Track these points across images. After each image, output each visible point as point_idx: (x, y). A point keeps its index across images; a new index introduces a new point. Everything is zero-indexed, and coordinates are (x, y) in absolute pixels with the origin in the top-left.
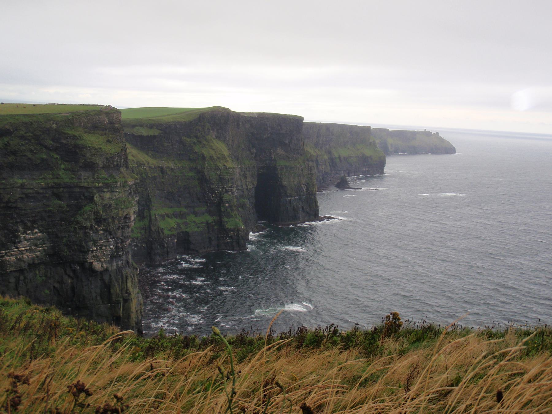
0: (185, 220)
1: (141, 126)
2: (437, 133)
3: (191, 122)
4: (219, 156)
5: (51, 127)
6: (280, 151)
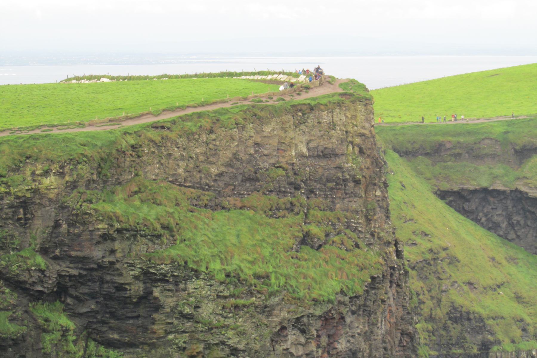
5: (36, 191)
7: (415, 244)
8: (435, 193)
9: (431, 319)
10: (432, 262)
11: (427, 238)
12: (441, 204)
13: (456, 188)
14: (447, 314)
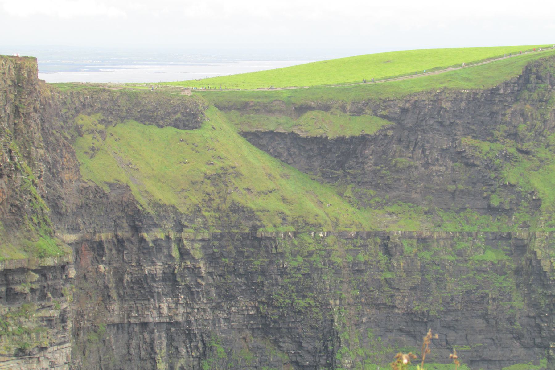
1: (327, 108)
3: (494, 91)
7: (213, 164)
8: (239, 133)
9: (218, 210)
10: (222, 175)
11: (221, 160)
12: (241, 140)
13: (253, 130)
14: (229, 207)
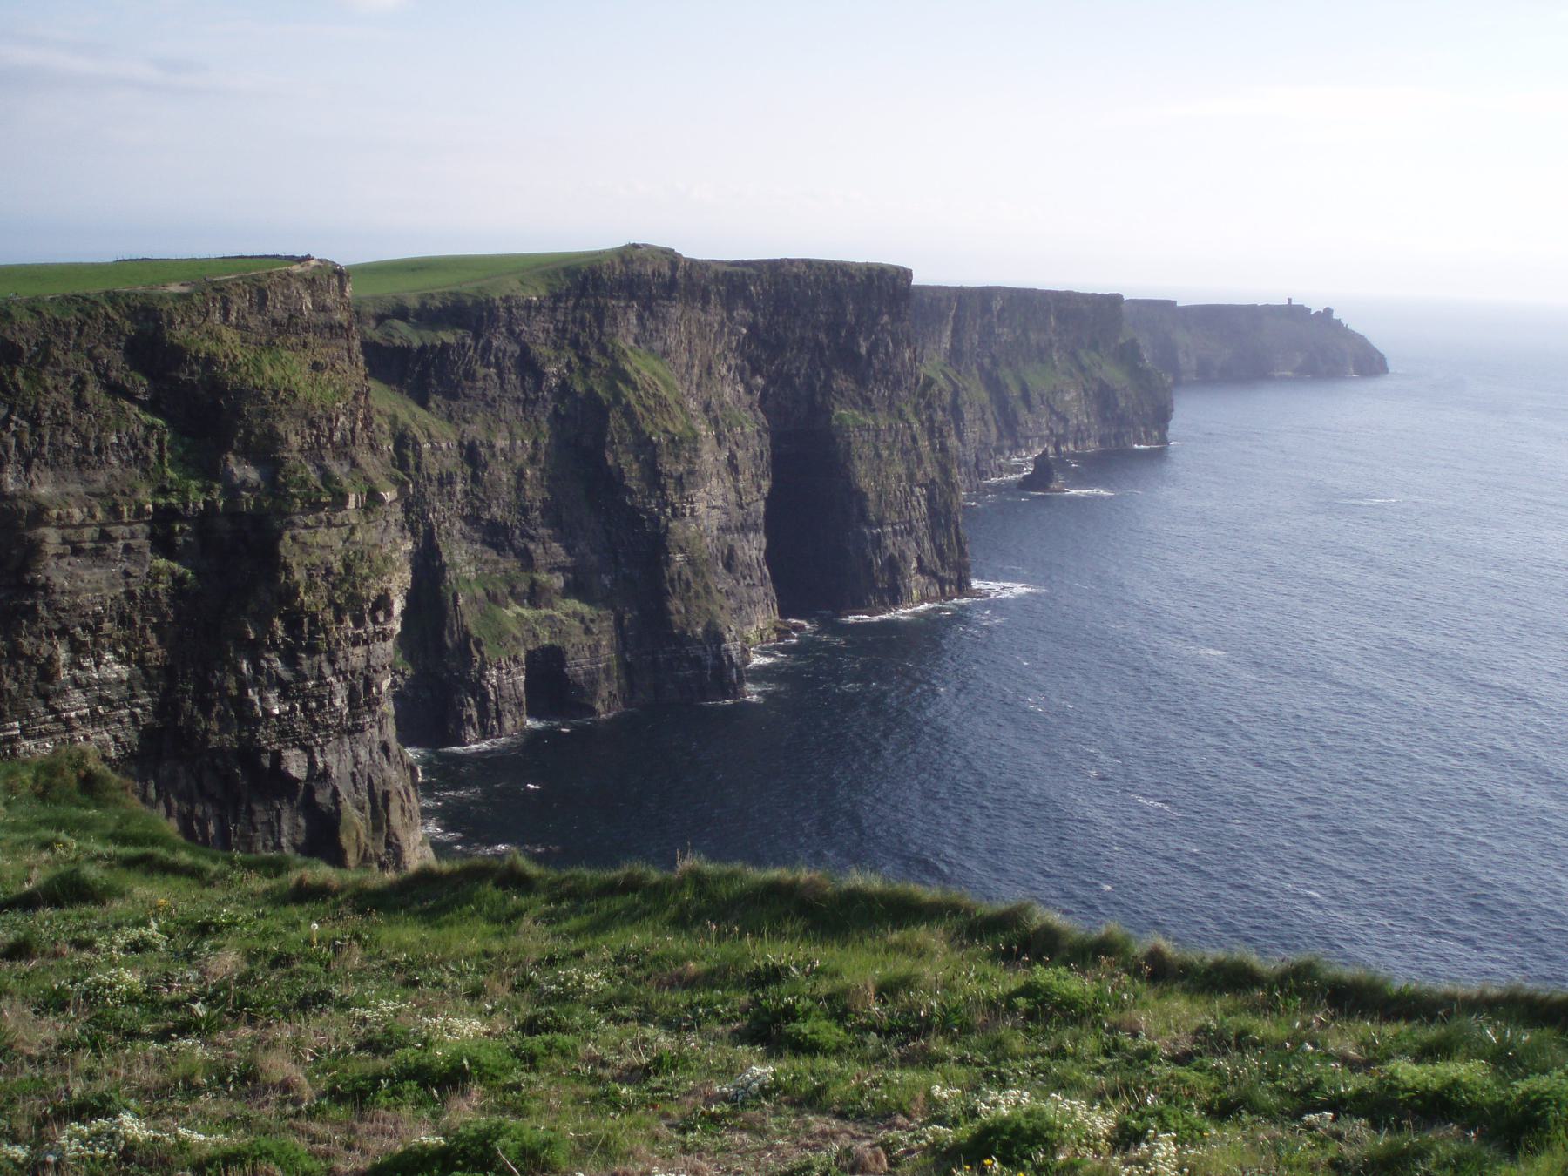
0: (549, 611)
2: (1328, 311)
4: (652, 403)
6: (842, 382)
